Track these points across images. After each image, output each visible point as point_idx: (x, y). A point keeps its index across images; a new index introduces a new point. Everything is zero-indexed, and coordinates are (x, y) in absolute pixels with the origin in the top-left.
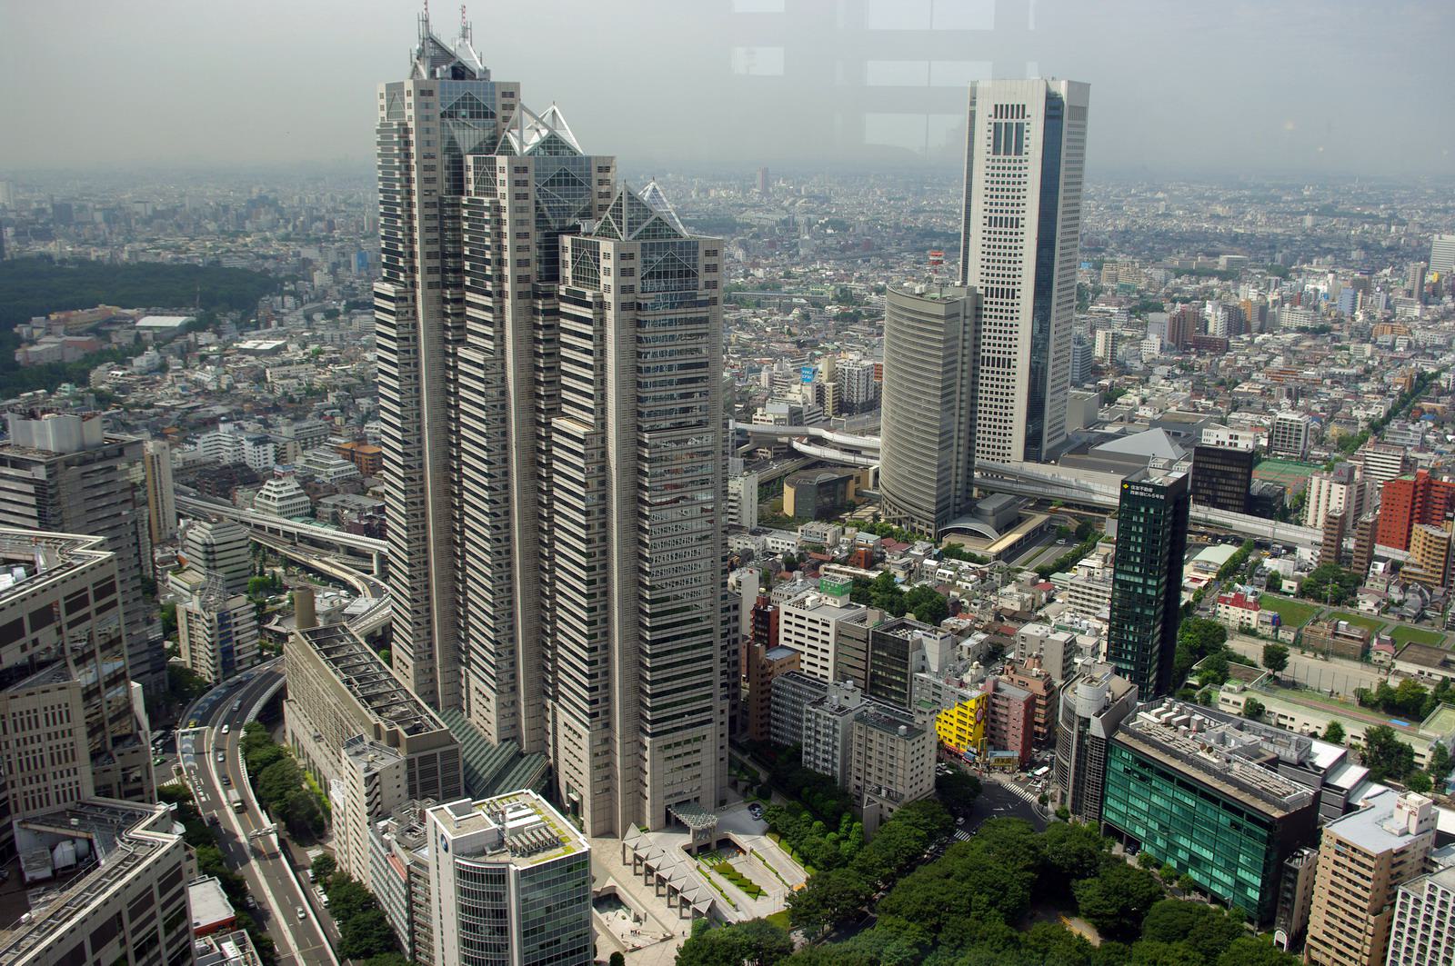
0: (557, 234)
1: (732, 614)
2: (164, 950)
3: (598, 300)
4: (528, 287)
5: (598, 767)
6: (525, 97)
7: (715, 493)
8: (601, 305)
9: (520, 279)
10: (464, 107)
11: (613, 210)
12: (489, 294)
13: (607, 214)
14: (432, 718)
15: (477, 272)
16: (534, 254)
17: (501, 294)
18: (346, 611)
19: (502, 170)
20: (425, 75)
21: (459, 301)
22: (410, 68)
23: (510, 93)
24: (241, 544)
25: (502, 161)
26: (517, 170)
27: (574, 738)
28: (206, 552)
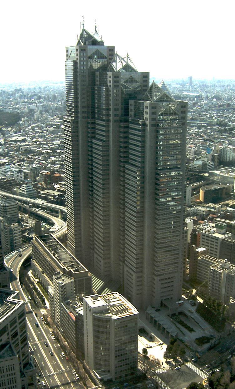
0: (129, 99)
1: (185, 234)
2: (19, 338)
3: (143, 123)
4: (118, 118)
5: (138, 286)
6: (118, 51)
7: (182, 192)
8: (144, 125)
9: (115, 115)
10: (96, 55)
11: (149, 91)
12: (104, 121)
13: (147, 92)
14: (82, 266)
15: (100, 113)
16: (119, 107)
17: (108, 121)
18: (51, 230)
19: (110, 77)
20: (83, 44)
21: (94, 123)
22: (77, 42)
23: (112, 50)
24: (14, 206)
25: (110, 74)
26: (115, 77)
27: (130, 276)
28: (4, 209)
